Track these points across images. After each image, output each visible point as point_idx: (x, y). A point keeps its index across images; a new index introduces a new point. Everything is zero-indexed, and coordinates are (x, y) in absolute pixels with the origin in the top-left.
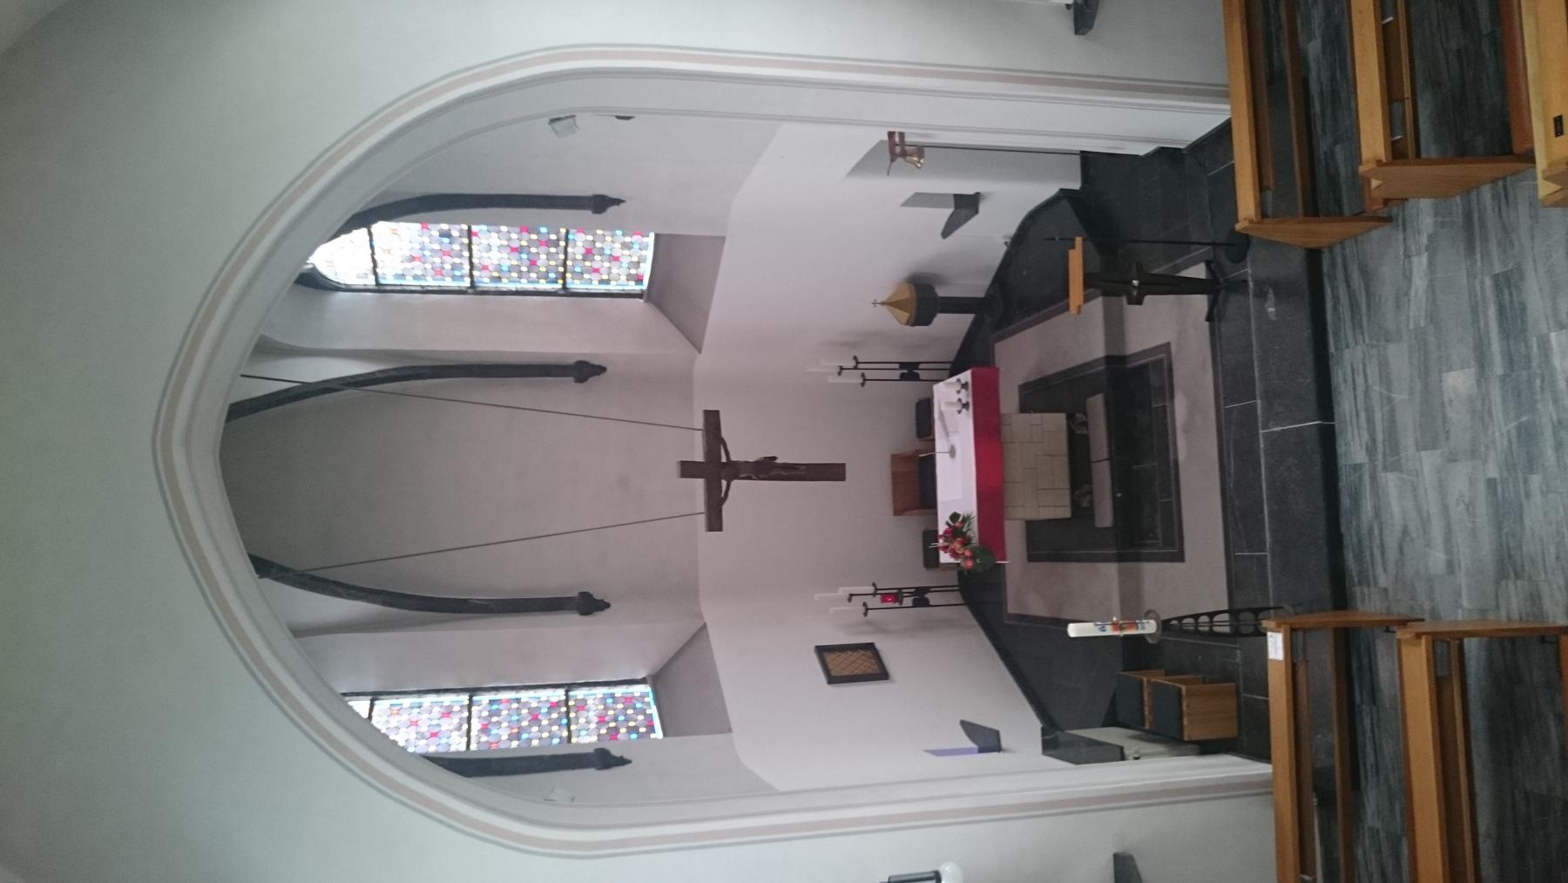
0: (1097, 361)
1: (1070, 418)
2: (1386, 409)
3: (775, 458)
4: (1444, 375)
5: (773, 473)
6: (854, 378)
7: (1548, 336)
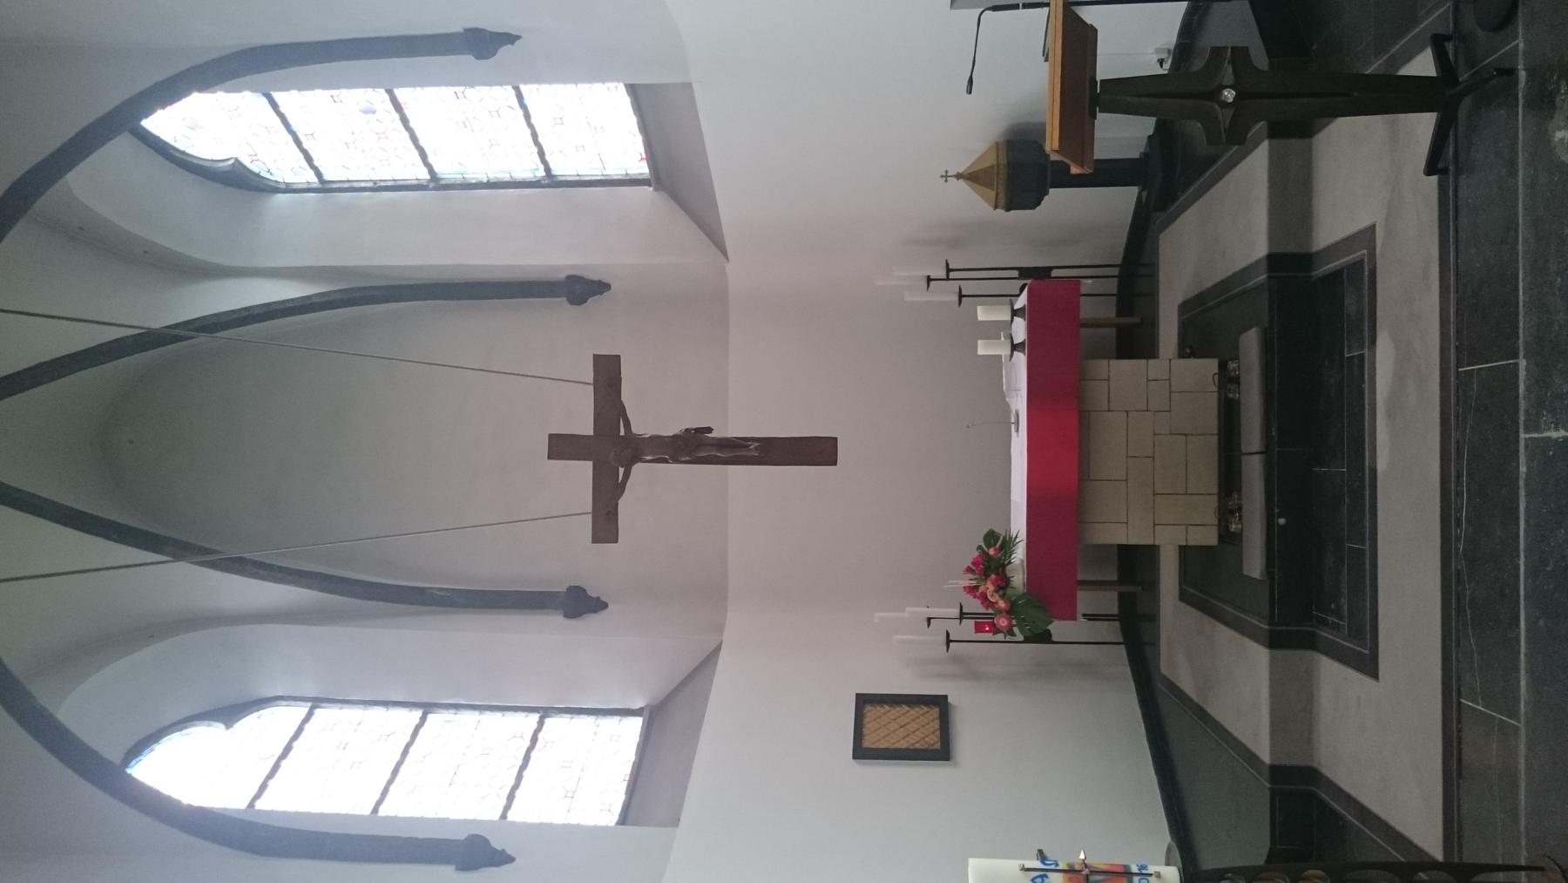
1: (1223, 366)
3: (709, 430)
6: (945, 294)
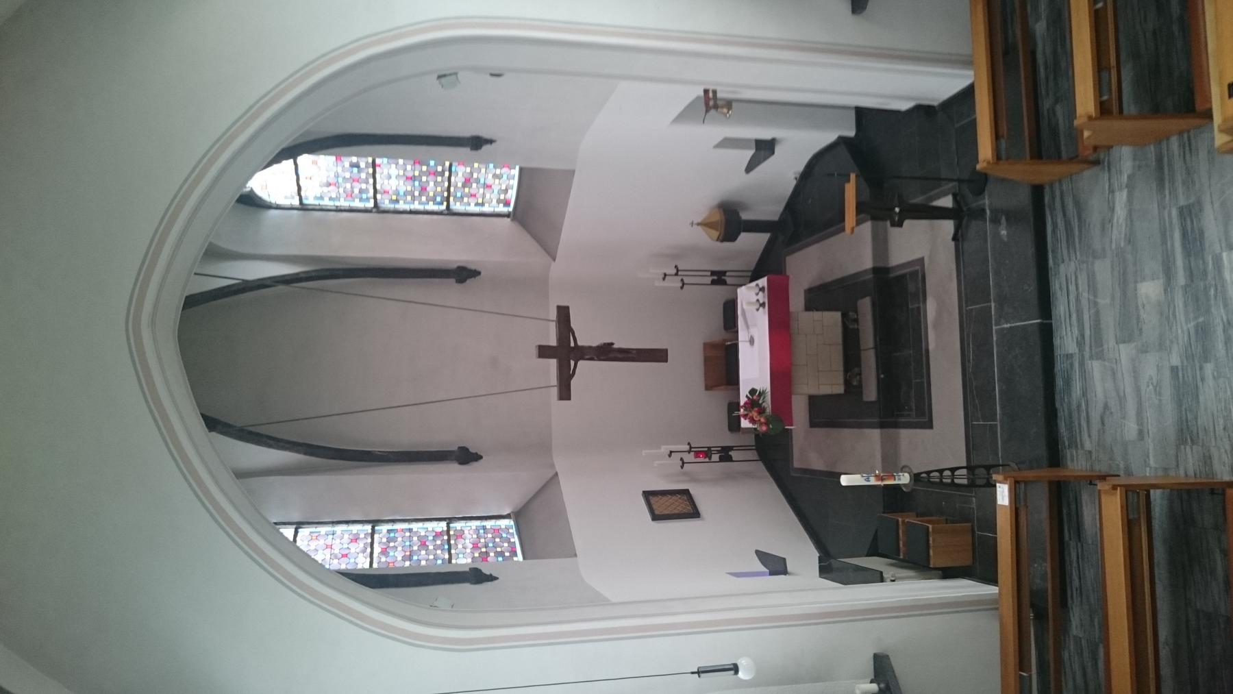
0: (866, 271)
1: (844, 316)
2: (1092, 311)
3: (612, 344)
4: (1138, 285)
5: (611, 355)
6: (675, 283)
7: (1220, 254)
